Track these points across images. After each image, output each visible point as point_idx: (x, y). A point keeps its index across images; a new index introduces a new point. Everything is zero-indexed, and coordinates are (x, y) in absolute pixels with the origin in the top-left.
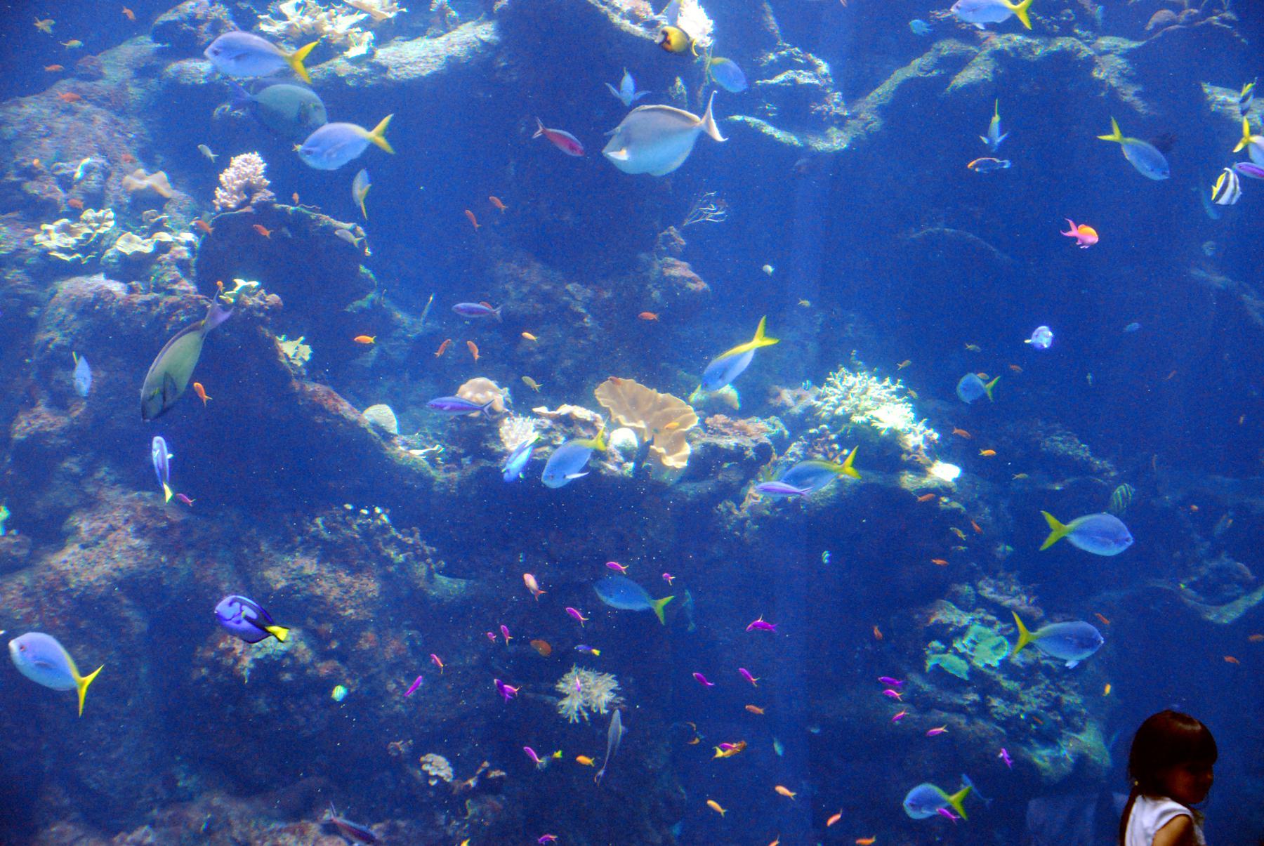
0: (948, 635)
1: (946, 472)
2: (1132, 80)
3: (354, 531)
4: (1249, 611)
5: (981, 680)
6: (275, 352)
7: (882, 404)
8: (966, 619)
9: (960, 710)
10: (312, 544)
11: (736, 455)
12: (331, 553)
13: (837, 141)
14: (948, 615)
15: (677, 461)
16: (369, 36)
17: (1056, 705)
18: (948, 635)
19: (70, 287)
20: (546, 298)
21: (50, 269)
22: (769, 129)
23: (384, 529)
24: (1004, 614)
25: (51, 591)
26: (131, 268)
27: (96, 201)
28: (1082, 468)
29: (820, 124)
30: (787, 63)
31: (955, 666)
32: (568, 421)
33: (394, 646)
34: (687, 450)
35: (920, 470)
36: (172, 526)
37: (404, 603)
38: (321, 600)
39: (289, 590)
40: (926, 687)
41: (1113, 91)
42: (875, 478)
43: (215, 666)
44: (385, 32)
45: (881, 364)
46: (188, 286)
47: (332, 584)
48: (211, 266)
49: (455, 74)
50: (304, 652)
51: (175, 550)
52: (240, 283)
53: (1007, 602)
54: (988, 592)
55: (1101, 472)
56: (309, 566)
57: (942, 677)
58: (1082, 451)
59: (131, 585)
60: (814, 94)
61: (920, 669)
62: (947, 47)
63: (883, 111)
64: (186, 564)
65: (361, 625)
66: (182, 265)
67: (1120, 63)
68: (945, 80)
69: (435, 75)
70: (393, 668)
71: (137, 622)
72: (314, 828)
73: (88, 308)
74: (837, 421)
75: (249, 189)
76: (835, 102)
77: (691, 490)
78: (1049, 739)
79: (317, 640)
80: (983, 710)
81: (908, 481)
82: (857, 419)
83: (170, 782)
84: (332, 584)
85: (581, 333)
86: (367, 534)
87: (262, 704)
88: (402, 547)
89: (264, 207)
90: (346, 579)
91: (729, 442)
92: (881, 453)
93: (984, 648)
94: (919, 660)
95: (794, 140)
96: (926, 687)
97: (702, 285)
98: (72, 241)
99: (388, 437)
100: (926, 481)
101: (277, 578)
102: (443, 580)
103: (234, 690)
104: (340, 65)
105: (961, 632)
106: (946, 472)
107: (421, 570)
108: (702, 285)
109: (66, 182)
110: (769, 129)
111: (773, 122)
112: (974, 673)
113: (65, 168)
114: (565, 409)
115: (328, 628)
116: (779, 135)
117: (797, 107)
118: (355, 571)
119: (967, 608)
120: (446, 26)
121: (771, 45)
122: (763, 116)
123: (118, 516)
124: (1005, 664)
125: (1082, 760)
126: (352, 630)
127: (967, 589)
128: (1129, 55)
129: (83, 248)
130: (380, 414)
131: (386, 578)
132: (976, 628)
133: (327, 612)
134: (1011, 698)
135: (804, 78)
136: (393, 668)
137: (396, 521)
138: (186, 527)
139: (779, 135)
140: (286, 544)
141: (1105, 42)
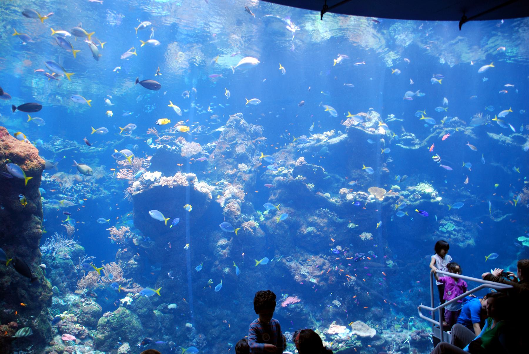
0: (443, 225)
1: (439, 199)
2: (472, 133)
3: (322, 212)
4: (503, 219)
5: (450, 233)
6: (306, 186)
7: (427, 188)
8: (446, 222)
9: (445, 237)
10: (316, 215)
11: (392, 197)
12: (319, 216)
13: (417, 147)
14: (443, 222)
15: (381, 199)
16: (327, 138)
17: (464, 236)
18: (443, 225)
19: (277, 178)
20: (360, 175)
21: (275, 176)
22: (402, 146)
23: (328, 212)
24: (455, 221)
25: (273, 222)
26: (285, 175)
27: (282, 166)
28: (469, 197)
29: (414, 145)
30: (406, 135)
31: (444, 230)
32: (359, 194)
33: (331, 229)
34: (383, 197)
35: (434, 198)
36: (292, 212)
37: (332, 223)
38: (317, 223)
39: (312, 222)
40: (439, 233)
41: (469, 136)
42: (426, 200)
43: (300, 233)
44: (330, 138)
45: (429, 181)
46: (291, 177)
47: (319, 220)
48: (295, 174)
49: (342, 142)
50: (315, 231)
51: (293, 216)
52: (299, 176)
53: (455, 219)
54: (452, 218)
55: (473, 197)
56: (316, 218)
57: (442, 232)
58: (468, 194)
59: (285, 221)
60: (412, 140)
61: (439, 231)
62: (438, 131)
63: (427, 142)
64: (295, 218)
65: (324, 227)
66: (291, 174)
67: (470, 131)
68: (438, 136)
69: (338, 143)
70: (330, 233)
71: (287, 227)
72: (318, 257)
73: (278, 181)
74: (420, 192)
75: (301, 162)
76: (417, 141)
77: (384, 204)
78: (463, 242)
79: (317, 229)
80: (449, 237)
81: (432, 200)
82: (422, 191)
83: (295, 250)
84: (319, 220)
85: (366, 180)
86: (324, 213)
87: (309, 239)
88: (331, 214)
89: (304, 165)
90: (321, 220)
91: (390, 196)
92: (427, 196)
93: (450, 227)
94: (438, 229)
95: (408, 148)
96: (439, 233)
97: (388, 171)
98: (277, 172)
99: (329, 198)
100: (435, 200)
101: (310, 220)
102: (339, 220)
103: (305, 236)
104: (322, 143)
105: (446, 225)
106: (439, 199)
107: (335, 218)
108: (388, 171)
109: (278, 164)
110: (402, 146)
111: (403, 145)
112: (448, 232)
113: (278, 162)
114: (358, 193)
115: (318, 227)
116: (404, 147)
117: (408, 142)
118: (323, 218)
119: (447, 220)
120: (340, 135)
121: (403, 132)
122: (401, 144)
123: (283, 211)
124: (454, 230)
125: (469, 245)
126: (322, 227)
127: (447, 217)
128: (472, 130)
129: (279, 173)
130: (328, 195)
131: (329, 219)
132: (449, 224)
133: (319, 225)
134: (454, 235)
135: (409, 137)
136: (330, 233)
137: (330, 210)
138: (295, 212)
139: (404, 147)
140: (312, 215)
141: (467, 128)
